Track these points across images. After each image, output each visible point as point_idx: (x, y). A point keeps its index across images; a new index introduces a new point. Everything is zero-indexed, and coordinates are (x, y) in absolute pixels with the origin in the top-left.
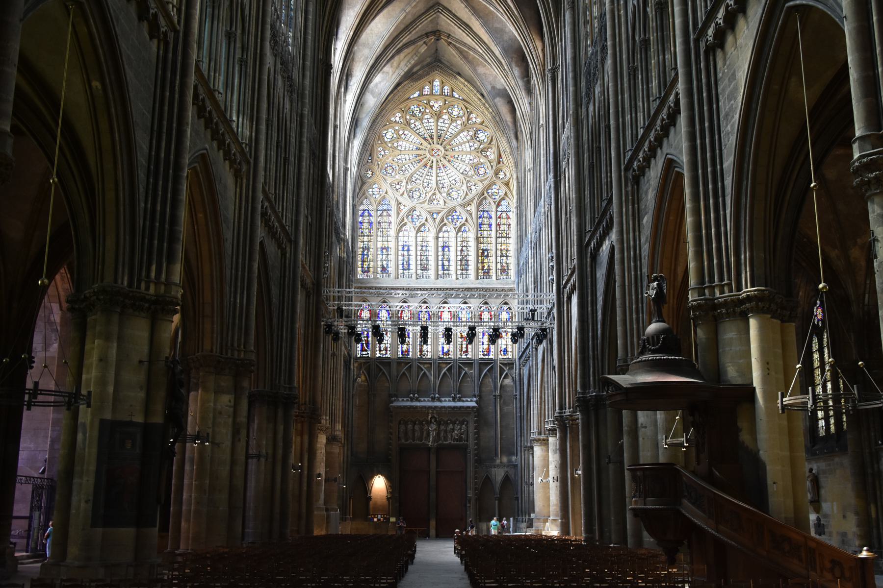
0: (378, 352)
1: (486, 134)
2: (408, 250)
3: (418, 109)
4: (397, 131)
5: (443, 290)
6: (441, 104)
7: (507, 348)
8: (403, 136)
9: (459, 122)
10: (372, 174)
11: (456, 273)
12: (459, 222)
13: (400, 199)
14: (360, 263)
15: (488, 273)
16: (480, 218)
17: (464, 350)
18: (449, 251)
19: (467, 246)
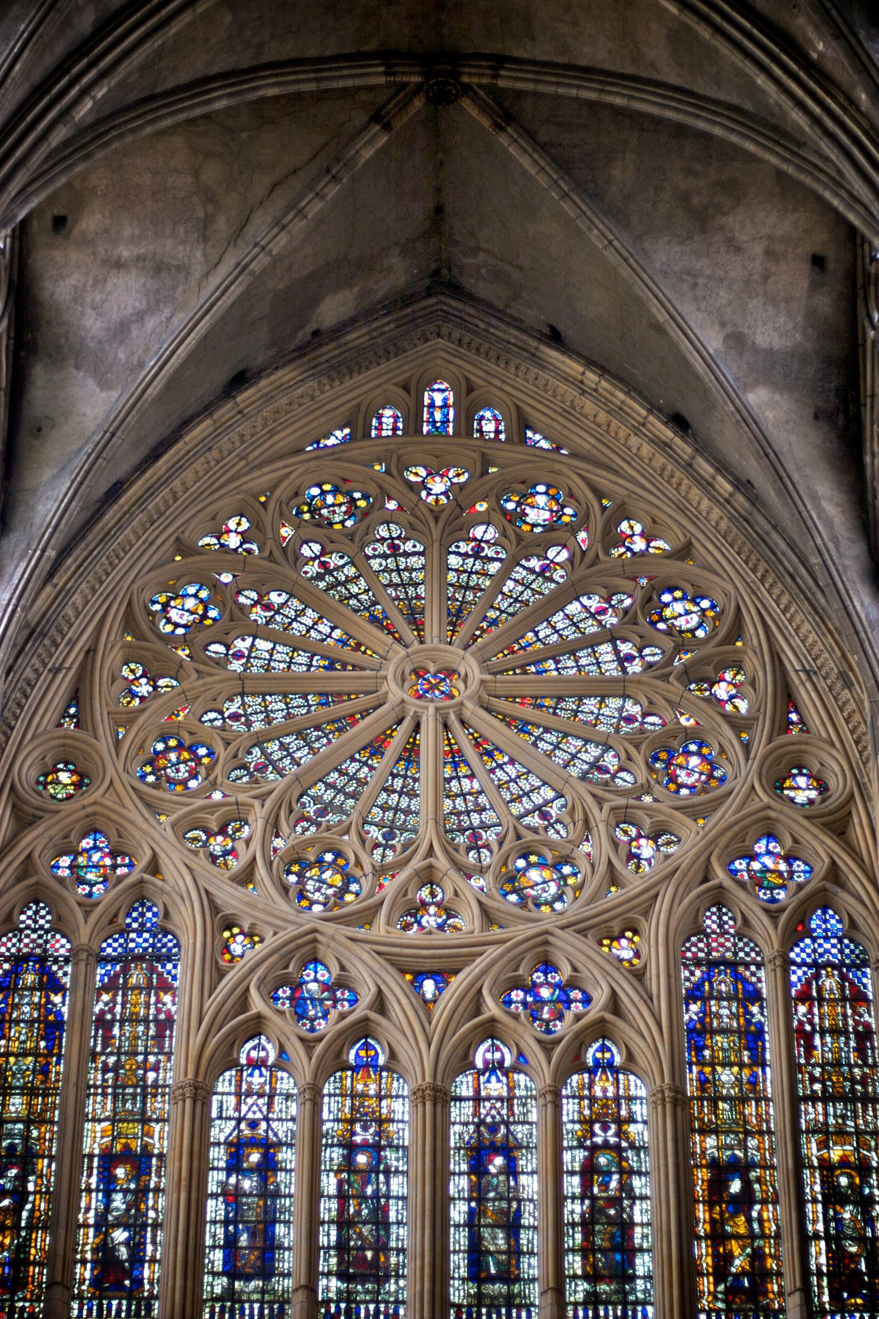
3: (340, 499)
6: (463, 479)
8: (258, 615)
10: (78, 785)
11: (558, 1290)
15: (758, 1290)
18: (511, 1170)
19: (618, 1148)
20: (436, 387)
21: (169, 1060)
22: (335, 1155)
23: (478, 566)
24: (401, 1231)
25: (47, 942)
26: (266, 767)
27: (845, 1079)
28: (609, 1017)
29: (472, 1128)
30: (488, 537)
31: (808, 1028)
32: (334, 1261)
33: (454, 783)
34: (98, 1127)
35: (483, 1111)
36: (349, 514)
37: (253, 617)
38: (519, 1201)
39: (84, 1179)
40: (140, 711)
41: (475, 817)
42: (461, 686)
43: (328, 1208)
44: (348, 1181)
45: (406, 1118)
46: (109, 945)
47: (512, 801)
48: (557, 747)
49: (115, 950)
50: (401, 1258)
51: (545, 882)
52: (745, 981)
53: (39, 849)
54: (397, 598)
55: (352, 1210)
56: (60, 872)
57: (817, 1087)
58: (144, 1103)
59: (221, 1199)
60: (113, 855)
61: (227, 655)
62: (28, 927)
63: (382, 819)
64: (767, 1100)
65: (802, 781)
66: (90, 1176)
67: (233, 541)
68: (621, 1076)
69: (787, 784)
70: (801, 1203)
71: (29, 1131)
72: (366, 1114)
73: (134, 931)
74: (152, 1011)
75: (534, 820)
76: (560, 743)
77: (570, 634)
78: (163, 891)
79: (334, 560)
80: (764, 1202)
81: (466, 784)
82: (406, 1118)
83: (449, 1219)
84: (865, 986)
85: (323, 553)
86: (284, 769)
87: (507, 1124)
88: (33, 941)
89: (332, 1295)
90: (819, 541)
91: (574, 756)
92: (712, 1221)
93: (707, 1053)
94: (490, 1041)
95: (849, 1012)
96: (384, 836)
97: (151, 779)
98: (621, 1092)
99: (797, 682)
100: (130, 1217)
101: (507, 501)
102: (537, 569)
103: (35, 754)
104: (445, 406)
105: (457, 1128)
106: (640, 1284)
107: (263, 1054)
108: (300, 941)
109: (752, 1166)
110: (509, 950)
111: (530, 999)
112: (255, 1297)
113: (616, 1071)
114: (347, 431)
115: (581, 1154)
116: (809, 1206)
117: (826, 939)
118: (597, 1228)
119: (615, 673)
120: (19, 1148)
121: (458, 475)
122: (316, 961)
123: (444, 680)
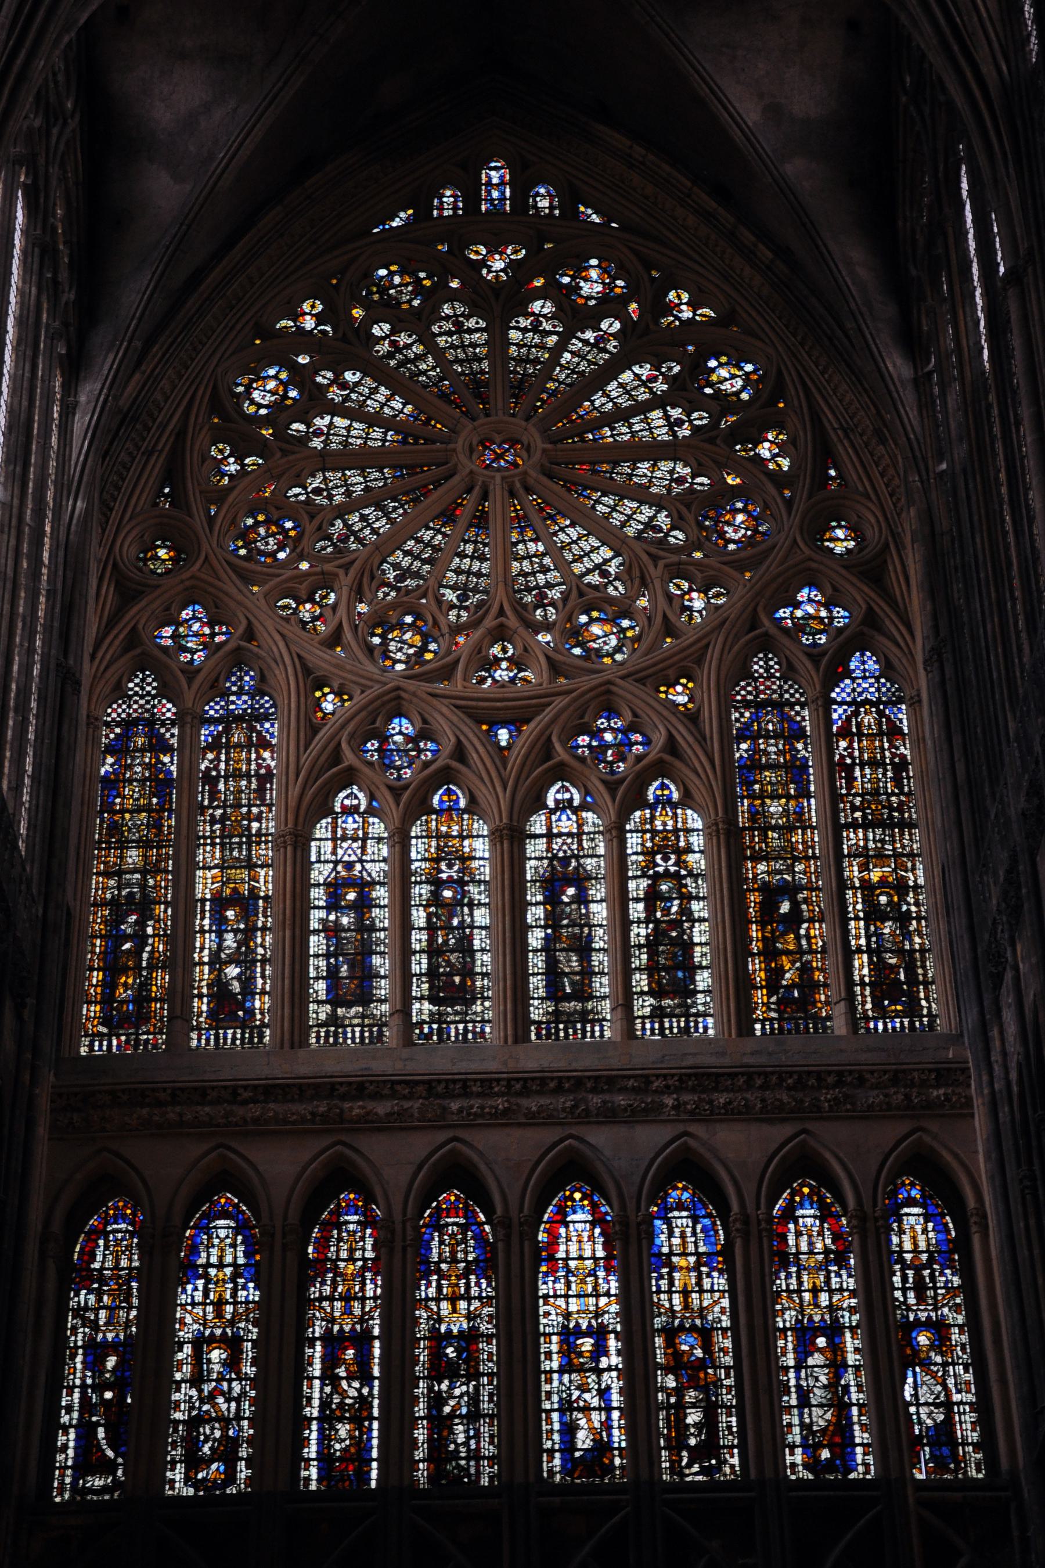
0: (177, 1474)
1: (749, 368)
2: (364, 904)
4: (300, 377)
5: (559, 1090)
7: (949, 1421)
9: (611, 325)
12: (631, 759)
13: (320, 659)
14: (96, 977)
15: (807, 1001)
16: (741, 737)
17: (692, 1442)
18: (581, 898)
19: (676, 876)
20: (493, 165)
21: (270, 811)
22: (423, 891)
23: (537, 340)
24: (485, 958)
25: (154, 706)
26: (348, 538)
27: (884, 807)
28: (667, 757)
29: (546, 862)
30: (546, 311)
31: (848, 761)
32: (426, 986)
33: (520, 546)
34: (209, 874)
35: (555, 846)
36: (415, 293)
37: (330, 396)
38: (591, 927)
39: (198, 922)
40: (229, 489)
41: (540, 577)
42: (525, 455)
43: (418, 939)
44: (436, 914)
45: (487, 855)
46: (212, 708)
47: (574, 561)
48: (614, 509)
49: (217, 711)
50: (486, 982)
51: (606, 636)
52: (791, 720)
53: (143, 621)
54: (463, 373)
55: (440, 940)
56: (163, 642)
57: (858, 814)
58: (249, 850)
59: (322, 934)
60: (211, 624)
61: (307, 432)
62: (136, 694)
63: (456, 583)
64: (813, 828)
65: (840, 533)
66: (202, 918)
67: (309, 323)
68: (679, 811)
69: (827, 536)
70: (844, 921)
71: (146, 880)
72: (450, 853)
73: (234, 693)
74: (253, 767)
75: (595, 579)
76: (616, 505)
77: (624, 402)
78: (259, 657)
79: (403, 339)
80: (812, 921)
81: (532, 547)
82: (487, 855)
83: (528, 945)
84: (901, 721)
85: (394, 331)
86: (364, 538)
87: (577, 857)
88: (141, 706)
89: (425, 1017)
90: (853, 305)
91: (630, 517)
92: (764, 939)
93: (757, 787)
94: (560, 784)
95: (886, 745)
96: (458, 597)
97: (243, 552)
98: (680, 825)
99: (835, 439)
100: (241, 954)
101: (562, 275)
102: (592, 341)
103: (134, 533)
104: (502, 183)
105: (533, 863)
106: (700, 998)
107: (355, 802)
108: (386, 698)
109: (802, 888)
110: (575, 700)
111: (594, 743)
112: (356, 1021)
113: (674, 806)
114: (410, 212)
115: (644, 883)
116: (852, 923)
117: (864, 678)
118: (661, 948)
119: (666, 438)
120: (138, 896)
121: (515, 252)
122: (400, 715)
123: (508, 450)
